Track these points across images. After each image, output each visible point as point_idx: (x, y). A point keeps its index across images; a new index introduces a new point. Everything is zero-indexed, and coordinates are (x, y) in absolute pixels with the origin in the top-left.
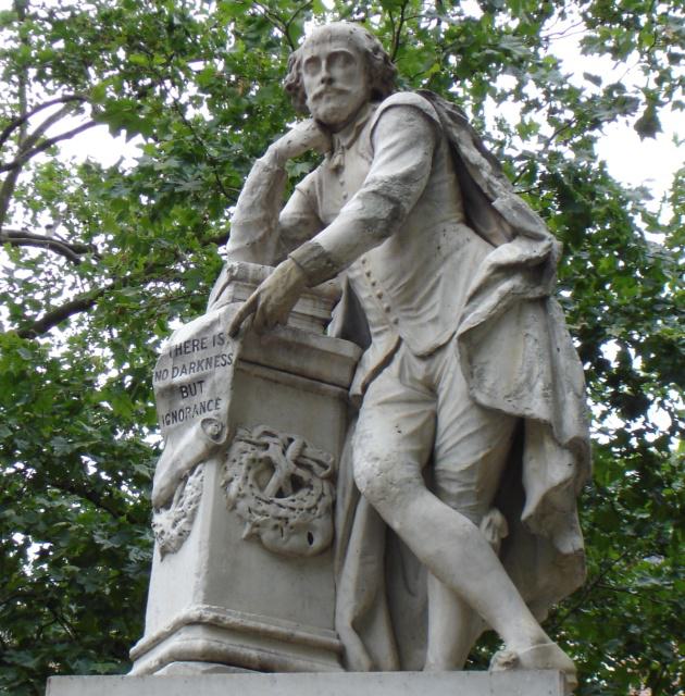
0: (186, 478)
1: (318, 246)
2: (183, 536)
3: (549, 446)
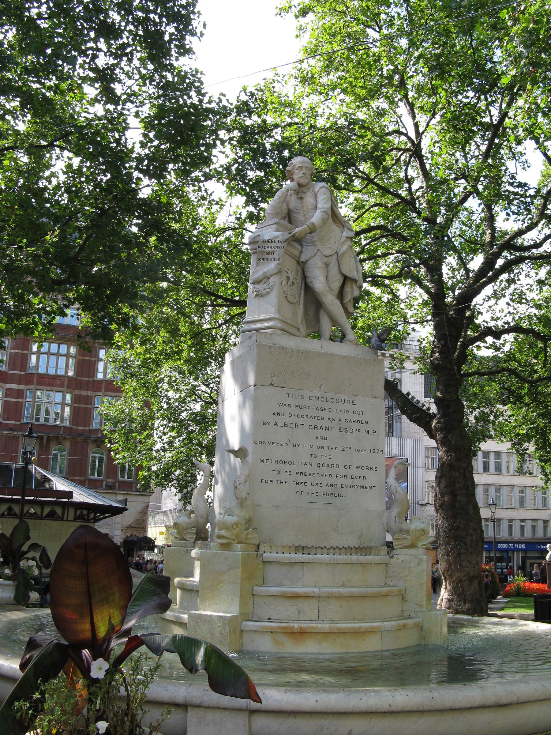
0: (269, 278)
1: (313, 224)
2: (267, 293)
3: (354, 286)
